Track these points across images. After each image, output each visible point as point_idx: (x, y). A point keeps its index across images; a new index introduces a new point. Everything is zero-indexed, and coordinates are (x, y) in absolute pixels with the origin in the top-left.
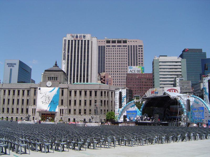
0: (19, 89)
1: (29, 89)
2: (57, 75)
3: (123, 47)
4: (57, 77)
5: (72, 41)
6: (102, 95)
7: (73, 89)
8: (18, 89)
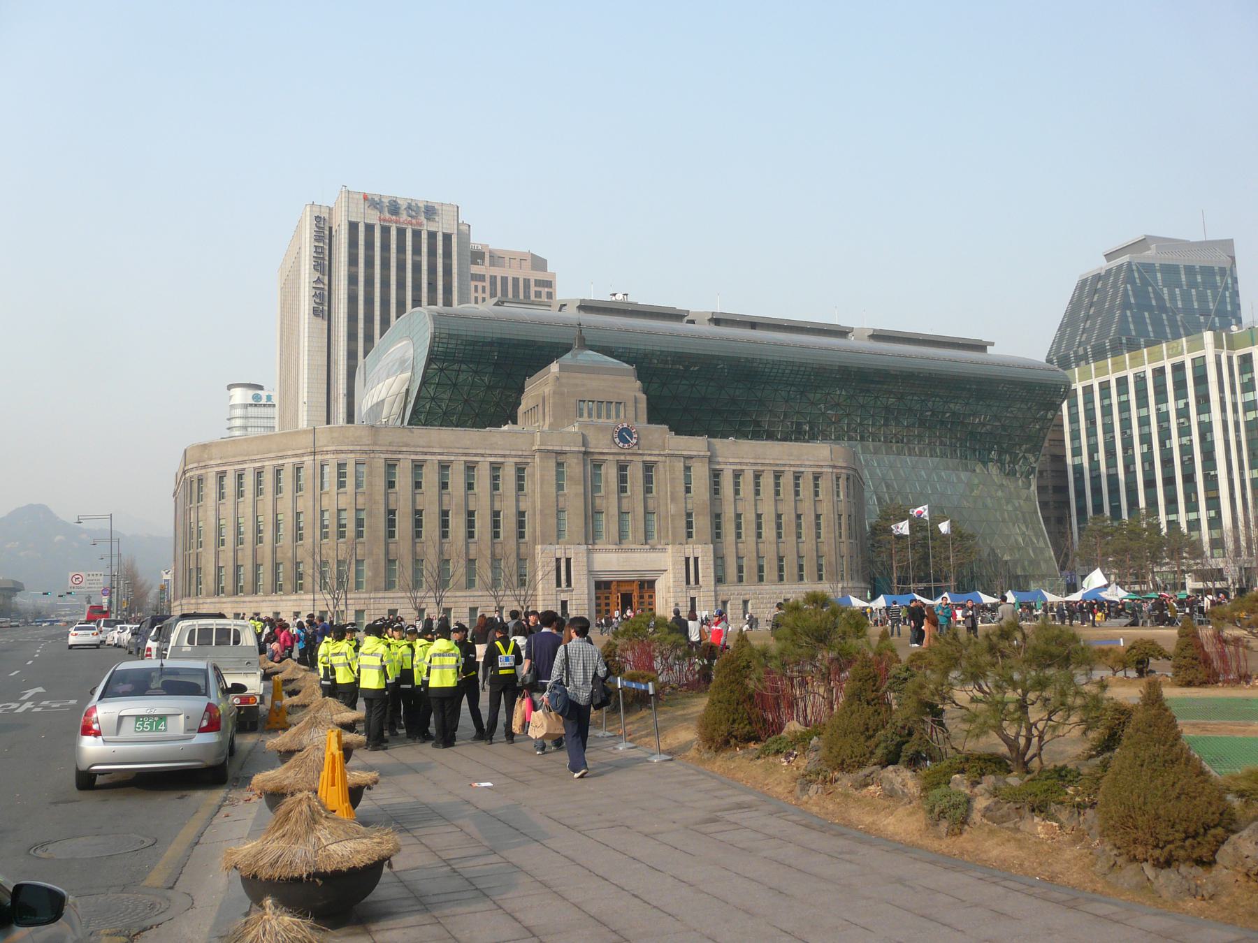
0: (476, 455)
1: (526, 457)
5: (370, 228)
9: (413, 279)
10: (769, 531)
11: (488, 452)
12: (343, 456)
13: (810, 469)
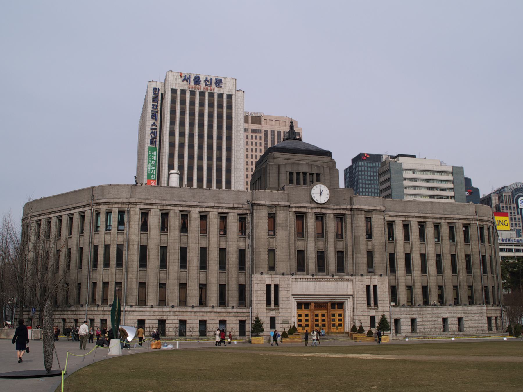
0: (208, 207)
2: (318, 167)
3: (252, 134)
4: (318, 175)
5: (183, 92)
6: (482, 241)
7: (400, 216)
8: (204, 210)
9: (209, 121)
10: (432, 268)
11: (216, 205)
12: (110, 206)
13: (461, 221)
